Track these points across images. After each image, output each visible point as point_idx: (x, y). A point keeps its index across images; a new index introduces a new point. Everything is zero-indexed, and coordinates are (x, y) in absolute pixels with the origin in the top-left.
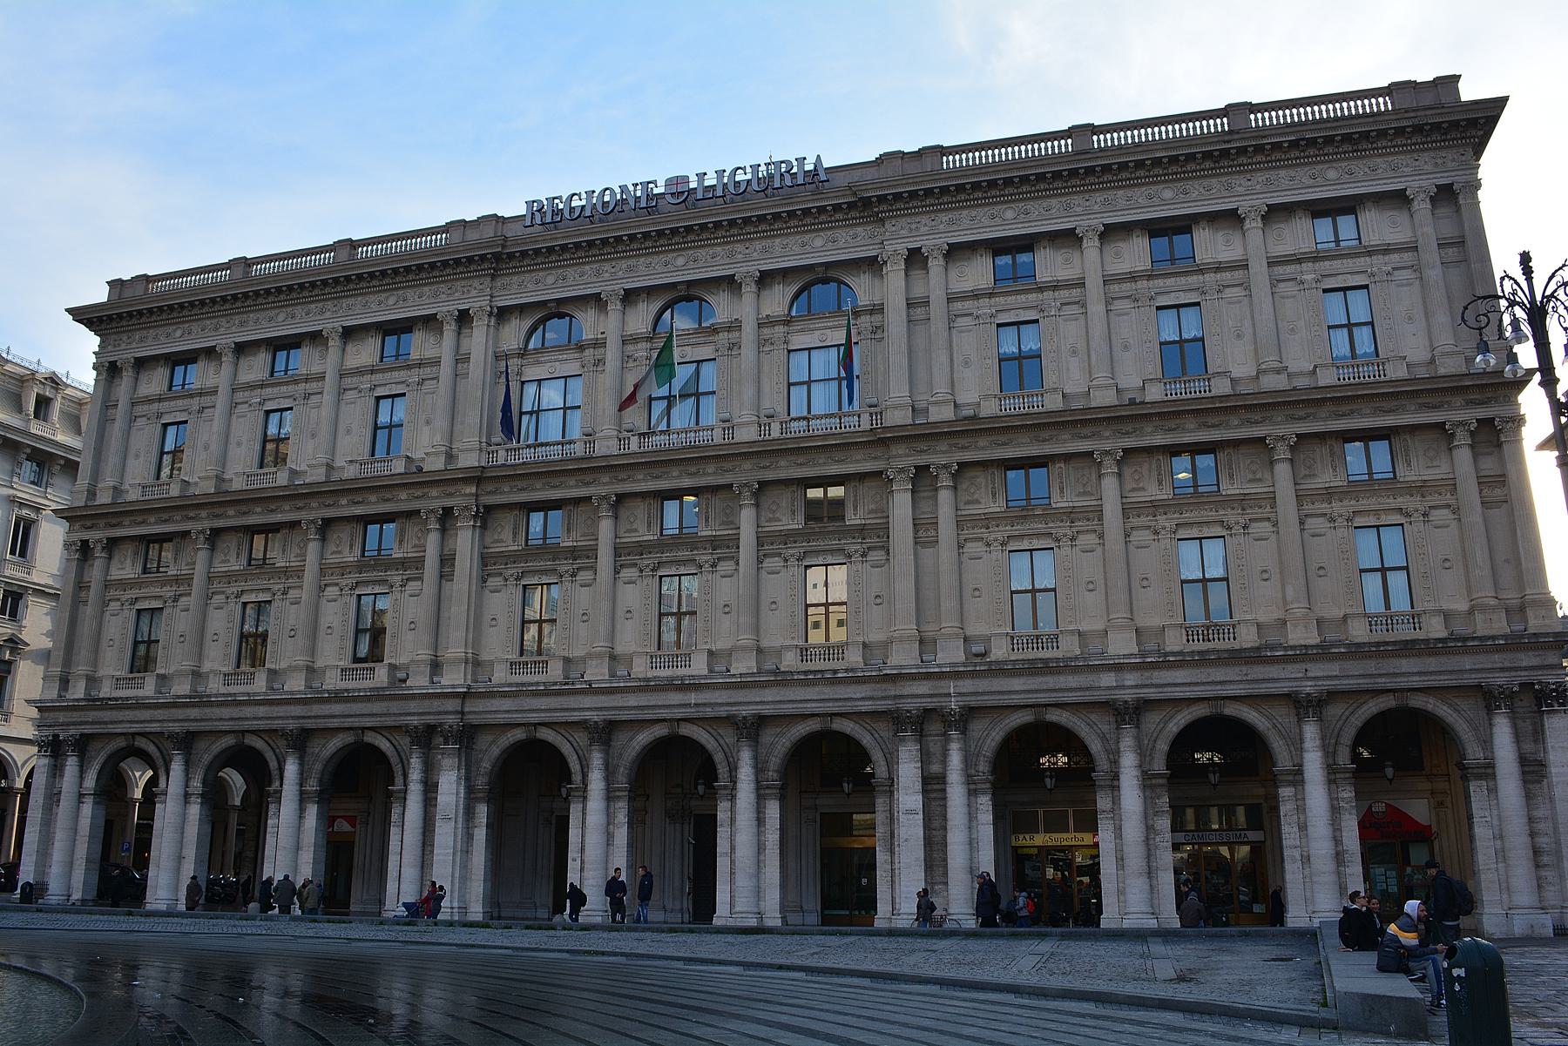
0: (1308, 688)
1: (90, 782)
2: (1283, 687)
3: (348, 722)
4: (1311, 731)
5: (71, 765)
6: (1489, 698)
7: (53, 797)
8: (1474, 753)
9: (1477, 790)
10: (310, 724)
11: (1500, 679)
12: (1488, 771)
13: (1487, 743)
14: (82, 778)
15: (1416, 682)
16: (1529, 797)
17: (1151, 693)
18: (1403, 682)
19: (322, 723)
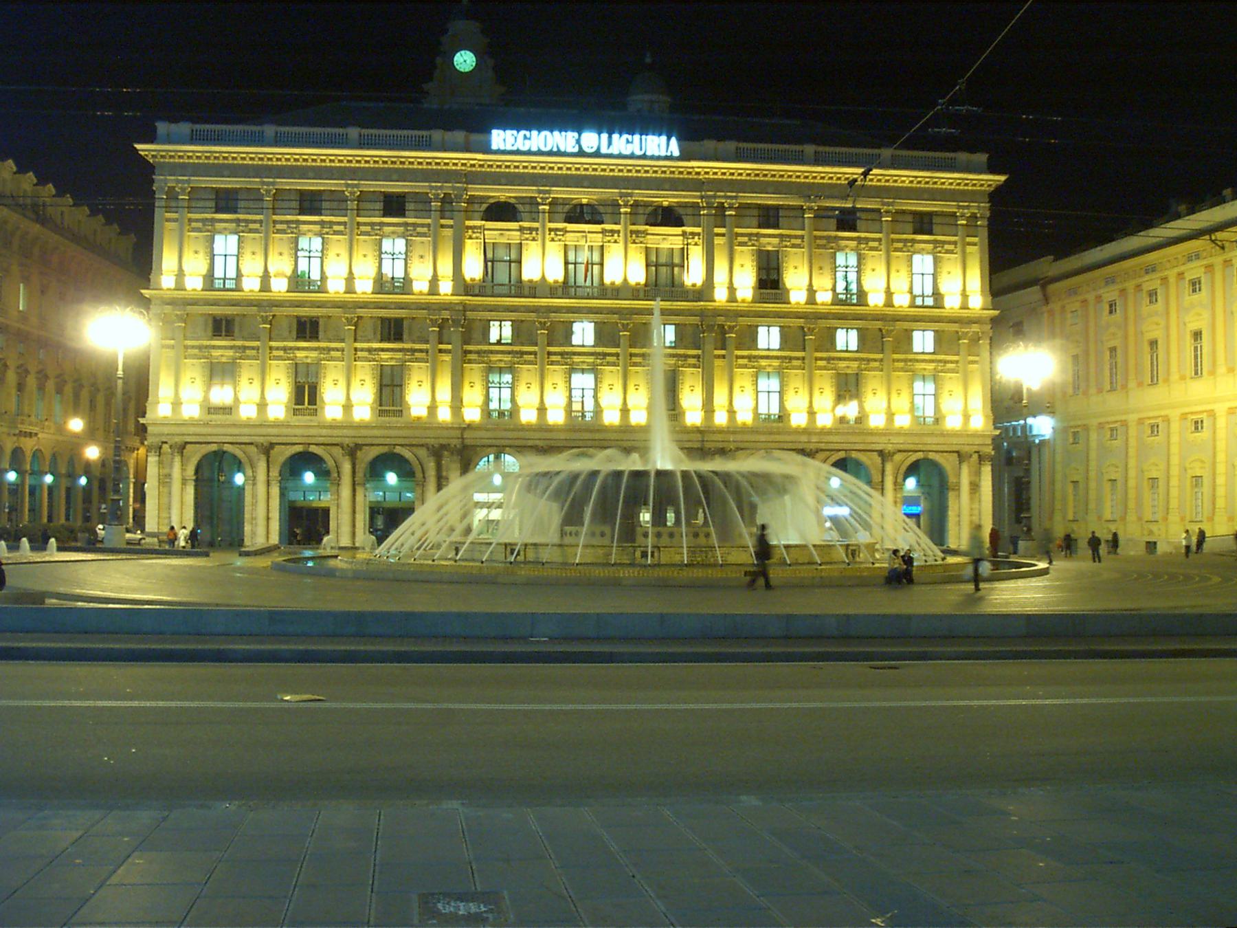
0: (890, 447)
1: (191, 471)
2: (879, 447)
3: (388, 441)
4: (889, 468)
5: (177, 459)
6: (961, 456)
7: (165, 480)
8: (952, 479)
9: (951, 496)
10: (360, 441)
11: (967, 449)
12: (957, 488)
13: (959, 475)
14: (183, 470)
15: (934, 448)
16: (972, 499)
17: (823, 446)
18: (929, 448)
19: (369, 441)
